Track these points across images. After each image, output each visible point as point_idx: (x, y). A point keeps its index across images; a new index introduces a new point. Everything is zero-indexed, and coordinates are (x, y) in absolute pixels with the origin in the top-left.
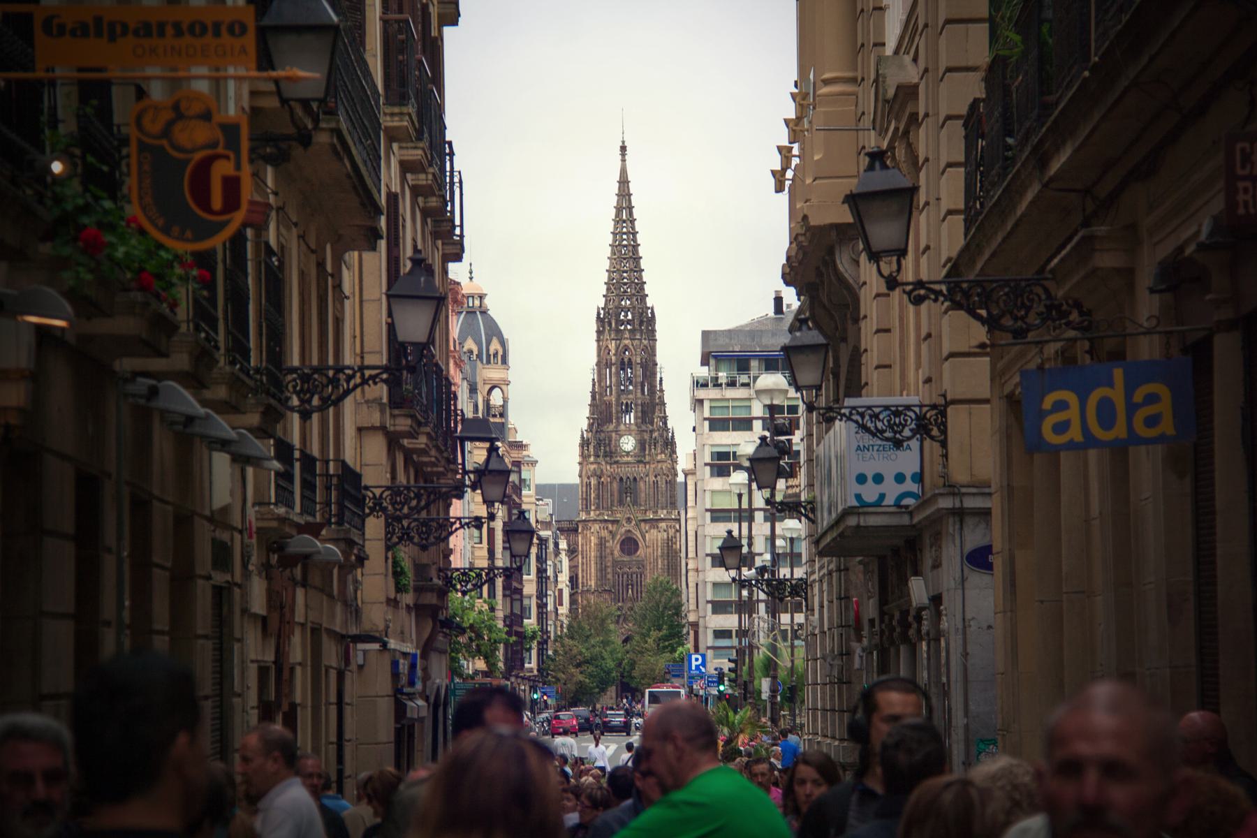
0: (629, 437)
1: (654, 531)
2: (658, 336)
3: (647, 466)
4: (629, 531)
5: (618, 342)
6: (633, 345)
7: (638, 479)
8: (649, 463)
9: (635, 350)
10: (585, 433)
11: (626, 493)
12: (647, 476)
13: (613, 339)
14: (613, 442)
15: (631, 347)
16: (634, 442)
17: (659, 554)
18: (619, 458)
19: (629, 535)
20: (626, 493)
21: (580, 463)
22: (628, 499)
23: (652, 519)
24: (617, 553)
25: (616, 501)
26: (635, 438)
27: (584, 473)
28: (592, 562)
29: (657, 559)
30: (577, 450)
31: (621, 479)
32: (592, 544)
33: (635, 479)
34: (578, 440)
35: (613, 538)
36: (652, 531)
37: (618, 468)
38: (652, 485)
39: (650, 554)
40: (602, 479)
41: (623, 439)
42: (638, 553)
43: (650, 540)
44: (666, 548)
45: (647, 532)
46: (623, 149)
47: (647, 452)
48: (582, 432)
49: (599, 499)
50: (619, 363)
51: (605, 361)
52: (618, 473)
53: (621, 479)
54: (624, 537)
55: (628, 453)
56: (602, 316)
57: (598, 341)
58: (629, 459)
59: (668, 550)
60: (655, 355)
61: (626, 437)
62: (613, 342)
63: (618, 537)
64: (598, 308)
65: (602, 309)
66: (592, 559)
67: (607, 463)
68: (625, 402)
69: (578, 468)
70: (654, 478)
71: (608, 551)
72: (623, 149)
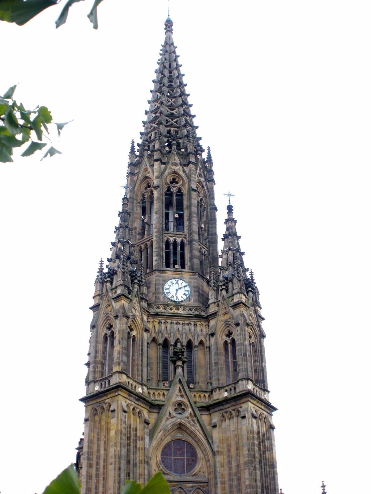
0: (180, 281)
1: (230, 425)
2: (215, 177)
3: (212, 322)
4: (181, 427)
5: (163, 166)
6: (184, 171)
7: (196, 343)
8: (215, 314)
9: (188, 177)
10: (106, 263)
11: (174, 362)
12: (212, 335)
13: (157, 160)
14: (152, 289)
15: (181, 173)
16: (187, 288)
17: (242, 460)
18: (161, 310)
19: (179, 436)
20: (174, 362)
21: (95, 308)
22: (179, 370)
23: (226, 401)
24: (156, 457)
25: (155, 378)
26: (189, 283)
27: (101, 322)
28: (111, 467)
29: (238, 472)
30: (91, 290)
31: (166, 343)
32: (112, 433)
33: (190, 344)
34: (94, 274)
35: (151, 435)
36: (224, 424)
37: (160, 323)
38: (222, 350)
39: (222, 466)
40: (134, 333)
41: (169, 283)
42: (197, 468)
43: (221, 441)
44: (257, 448)
45: (215, 426)
46: (169, 25)
47: (210, 302)
48: (101, 263)
49: (128, 356)
50: (165, 190)
51: (140, 198)
52: (160, 331)
53: (166, 342)
54: (168, 439)
55: (177, 304)
56: (137, 154)
57: (131, 174)
58: (181, 311)
59: (260, 455)
60: (213, 198)
61: (174, 281)
62: (157, 164)
63: (159, 435)
64: (133, 142)
65: (138, 145)
66: (111, 460)
67: (142, 308)
68: (171, 240)
69: (91, 314)
70: (225, 338)
71: (140, 456)
72: (169, 25)
